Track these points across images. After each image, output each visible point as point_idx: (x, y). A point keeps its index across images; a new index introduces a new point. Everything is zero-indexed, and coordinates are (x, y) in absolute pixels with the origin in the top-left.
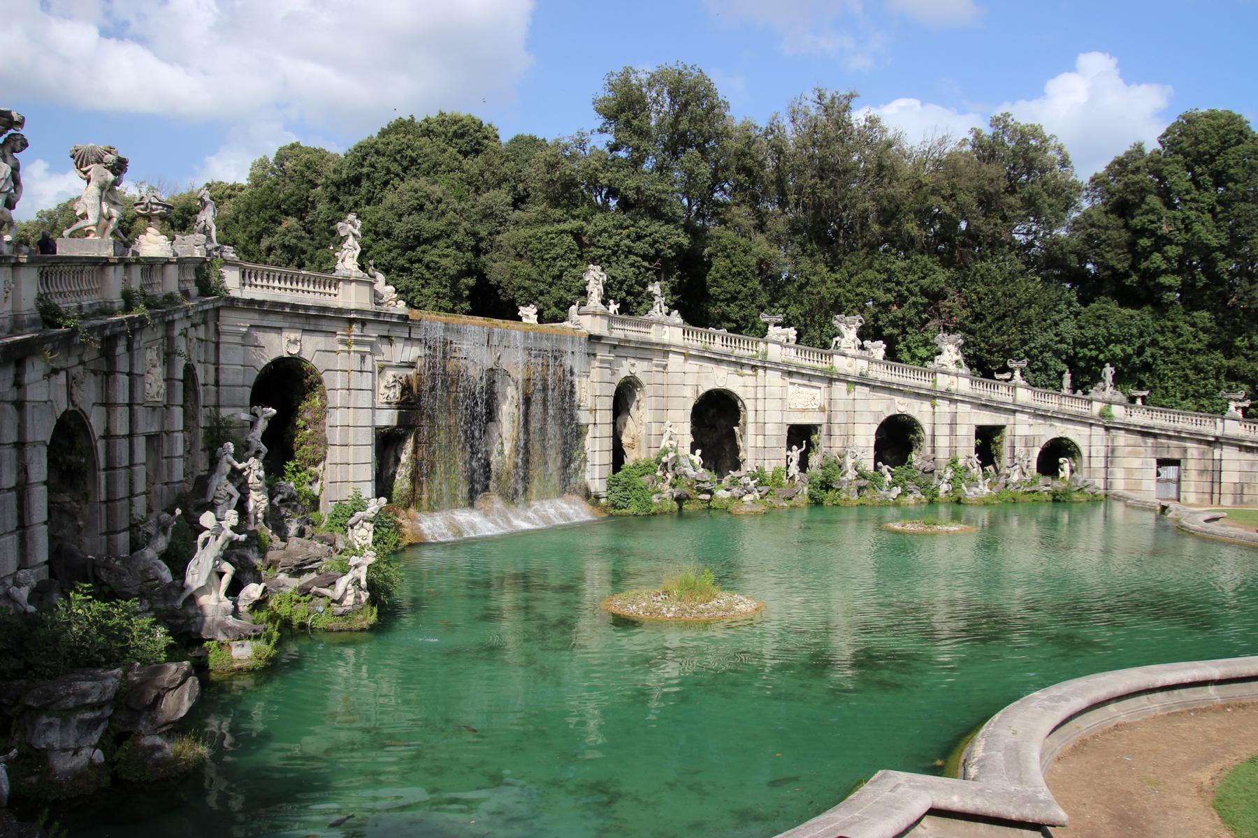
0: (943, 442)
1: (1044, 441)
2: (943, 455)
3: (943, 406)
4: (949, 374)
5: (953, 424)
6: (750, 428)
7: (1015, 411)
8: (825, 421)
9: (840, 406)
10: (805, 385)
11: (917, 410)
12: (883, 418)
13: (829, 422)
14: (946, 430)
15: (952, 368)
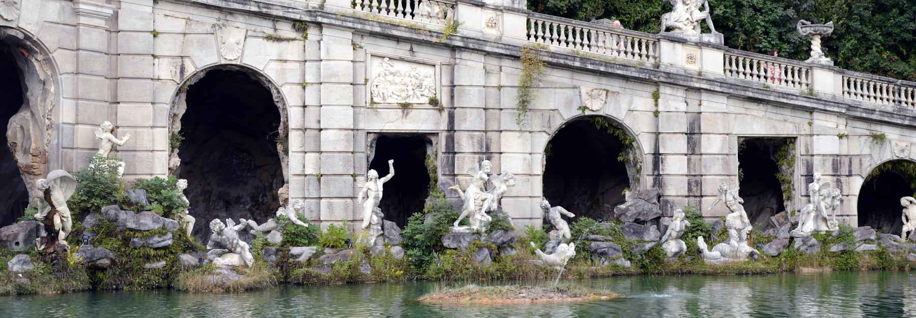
0: (675, 166)
1: (868, 168)
2: (675, 188)
3: (673, 101)
4: (683, 42)
5: (693, 134)
6: (295, 141)
7: (811, 111)
8: (444, 126)
9: (471, 98)
10: (401, 60)
11: (624, 106)
12: (558, 123)
13: (451, 129)
14: (681, 144)
15: (692, 33)
